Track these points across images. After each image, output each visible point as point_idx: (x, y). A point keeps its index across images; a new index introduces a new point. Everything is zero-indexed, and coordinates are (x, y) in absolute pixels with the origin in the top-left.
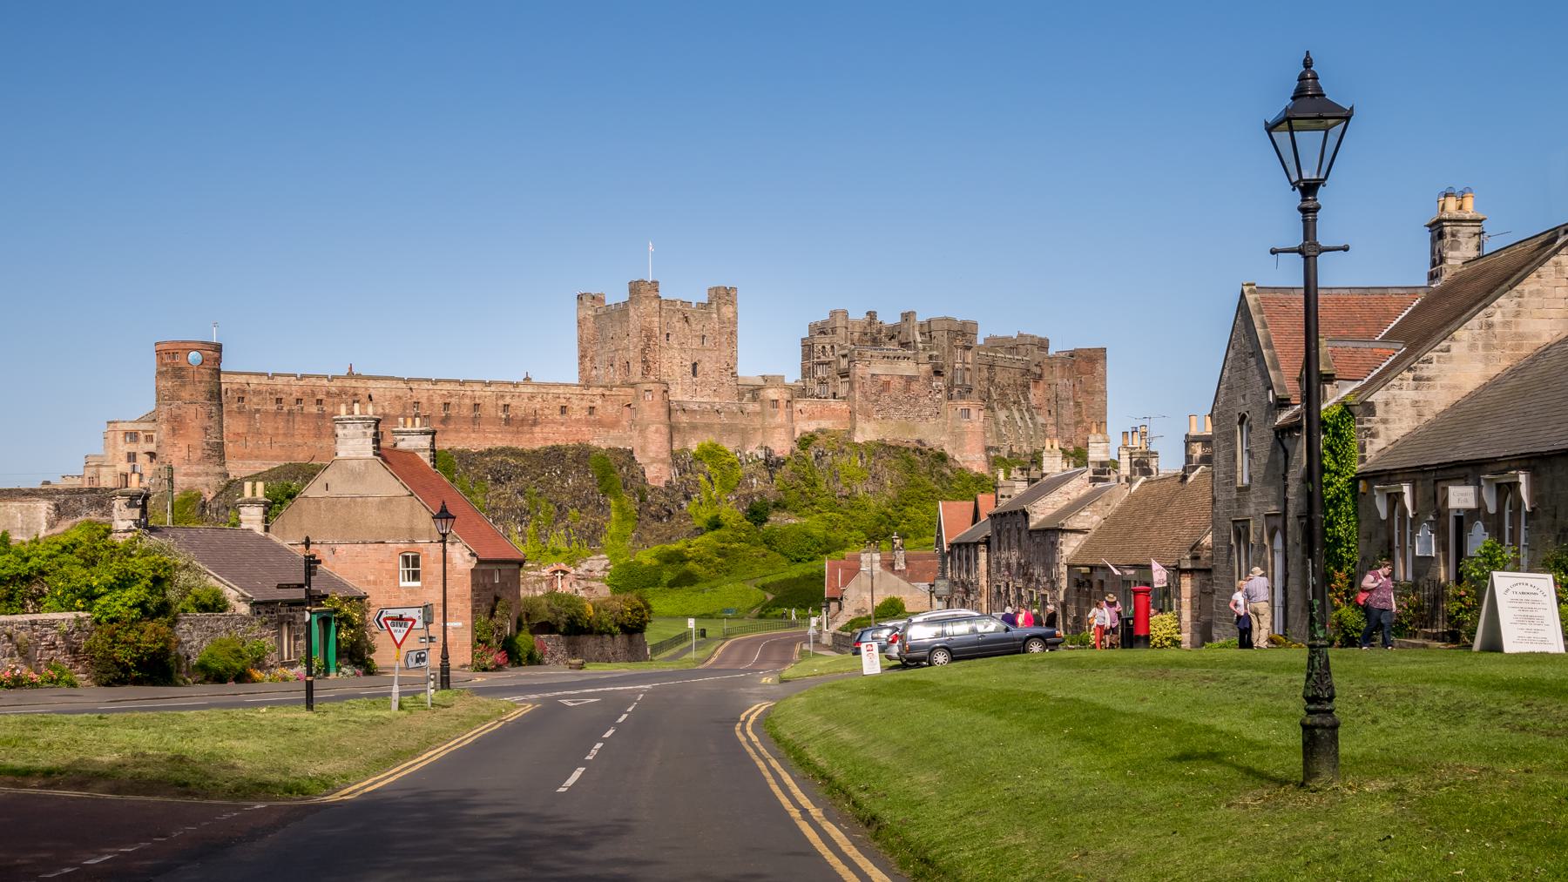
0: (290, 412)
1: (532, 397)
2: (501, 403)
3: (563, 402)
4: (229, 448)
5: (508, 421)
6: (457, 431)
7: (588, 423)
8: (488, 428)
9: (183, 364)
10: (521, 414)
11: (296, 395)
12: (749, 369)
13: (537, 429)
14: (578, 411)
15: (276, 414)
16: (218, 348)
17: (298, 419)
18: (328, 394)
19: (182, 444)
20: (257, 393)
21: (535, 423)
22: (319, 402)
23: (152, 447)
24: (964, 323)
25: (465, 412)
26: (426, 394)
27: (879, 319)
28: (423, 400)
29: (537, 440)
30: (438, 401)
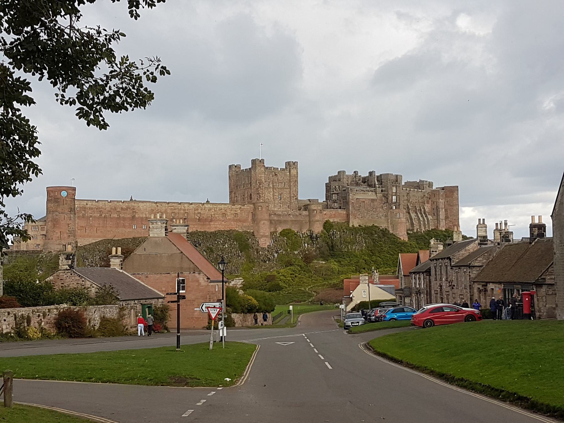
2: (196, 212)
5: (199, 220)
9: (59, 196)
10: (205, 216)
12: (303, 196)
13: (212, 223)
16: (74, 189)
19: (58, 231)
21: (211, 221)
23: (44, 233)
27: (359, 174)
29: (212, 228)
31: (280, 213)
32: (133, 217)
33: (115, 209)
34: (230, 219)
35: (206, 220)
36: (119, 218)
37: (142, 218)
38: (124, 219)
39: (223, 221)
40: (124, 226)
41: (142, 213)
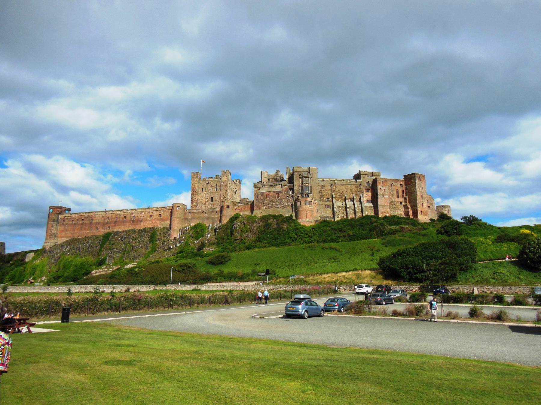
0: (75, 224)
1: (141, 213)
2: (132, 215)
3: (151, 213)
5: (133, 221)
6: (118, 225)
7: (158, 220)
10: (137, 218)
13: (142, 223)
14: (155, 216)
15: (71, 224)
18: (85, 217)
20: (67, 219)
21: (142, 221)
25: (121, 219)
28: (110, 217)
29: (141, 226)
30: (114, 217)
31: (195, 211)
32: (91, 223)
35: (138, 221)
36: (83, 224)
37: (96, 223)
38: (86, 224)
40: (85, 229)
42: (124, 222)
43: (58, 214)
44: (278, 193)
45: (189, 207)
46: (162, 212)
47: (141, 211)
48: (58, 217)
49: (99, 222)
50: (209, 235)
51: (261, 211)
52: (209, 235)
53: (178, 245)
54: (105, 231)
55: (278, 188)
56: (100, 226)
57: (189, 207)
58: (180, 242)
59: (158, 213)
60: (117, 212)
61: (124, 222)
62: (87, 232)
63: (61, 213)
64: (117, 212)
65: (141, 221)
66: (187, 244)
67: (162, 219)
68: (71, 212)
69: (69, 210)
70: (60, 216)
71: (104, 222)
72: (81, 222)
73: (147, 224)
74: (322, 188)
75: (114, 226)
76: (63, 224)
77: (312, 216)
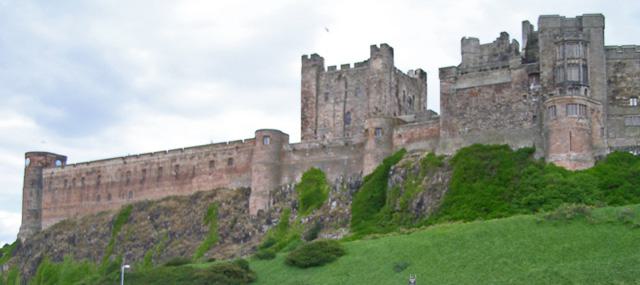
0: (70, 188)
1: (192, 158)
2: (174, 164)
3: (211, 157)
4: (44, 213)
6: (148, 188)
8: (167, 183)
10: (185, 170)
11: (73, 176)
13: (194, 180)
14: (221, 165)
15: (64, 189)
17: (73, 190)
18: (87, 173)
20: (57, 178)
21: (194, 175)
22: (83, 179)
24: (580, 19)
26: (133, 165)
28: (132, 170)
30: (139, 169)
32: (98, 183)
33: (80, 174)
34: (220, 170)
36: (83, 187)
37: (107, 184)
38: (89, 186)
39: (210, 174)
40: (88, 199)
41: (108, 177)
42: (159, 178)
43: (41, 169)
44: (499, 87)
45: (295, 137)
46: (235, 154)
47: (190, 152)
48: (40, 175)
49: (113, 183)
50: (334, 204)
51: (459, 140)
52: (334, 204)
53: (266, 228)
54: (125, 201)
55: (498, 77)
56: (114, 191)
57: (295, 137)
58: (269, 222)
59: (227, 156)
60: (146, 158)
61: (159, 178)
62: (90, 206)
63: (46, 165)
64: (146, 158)
65: (193, 174)
66: (285, 225)
67: (235, 170)
68: (68, 162)
69: (63, 159)
70: (46, 172)
71: (121, 182)
72: (79, 184)
73: (204, 184)
74: (617, 71)
75: (141, 189)
76: (50, 190)
77: (592, 147)
